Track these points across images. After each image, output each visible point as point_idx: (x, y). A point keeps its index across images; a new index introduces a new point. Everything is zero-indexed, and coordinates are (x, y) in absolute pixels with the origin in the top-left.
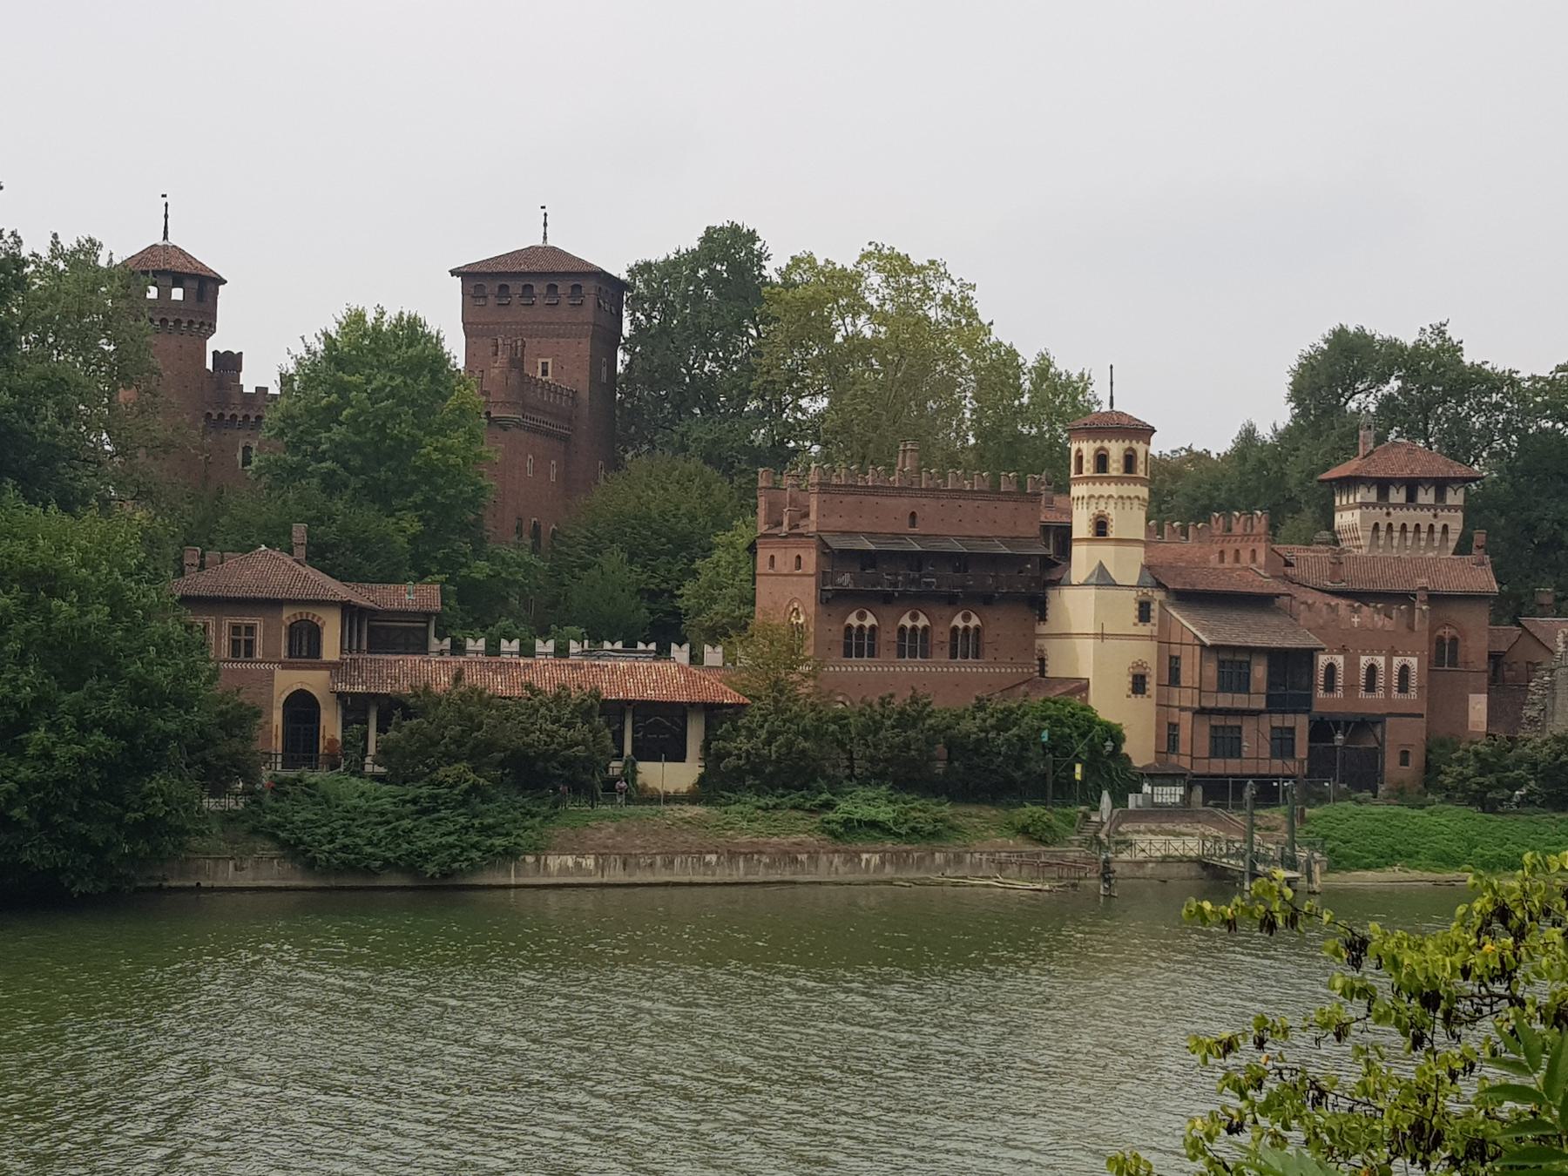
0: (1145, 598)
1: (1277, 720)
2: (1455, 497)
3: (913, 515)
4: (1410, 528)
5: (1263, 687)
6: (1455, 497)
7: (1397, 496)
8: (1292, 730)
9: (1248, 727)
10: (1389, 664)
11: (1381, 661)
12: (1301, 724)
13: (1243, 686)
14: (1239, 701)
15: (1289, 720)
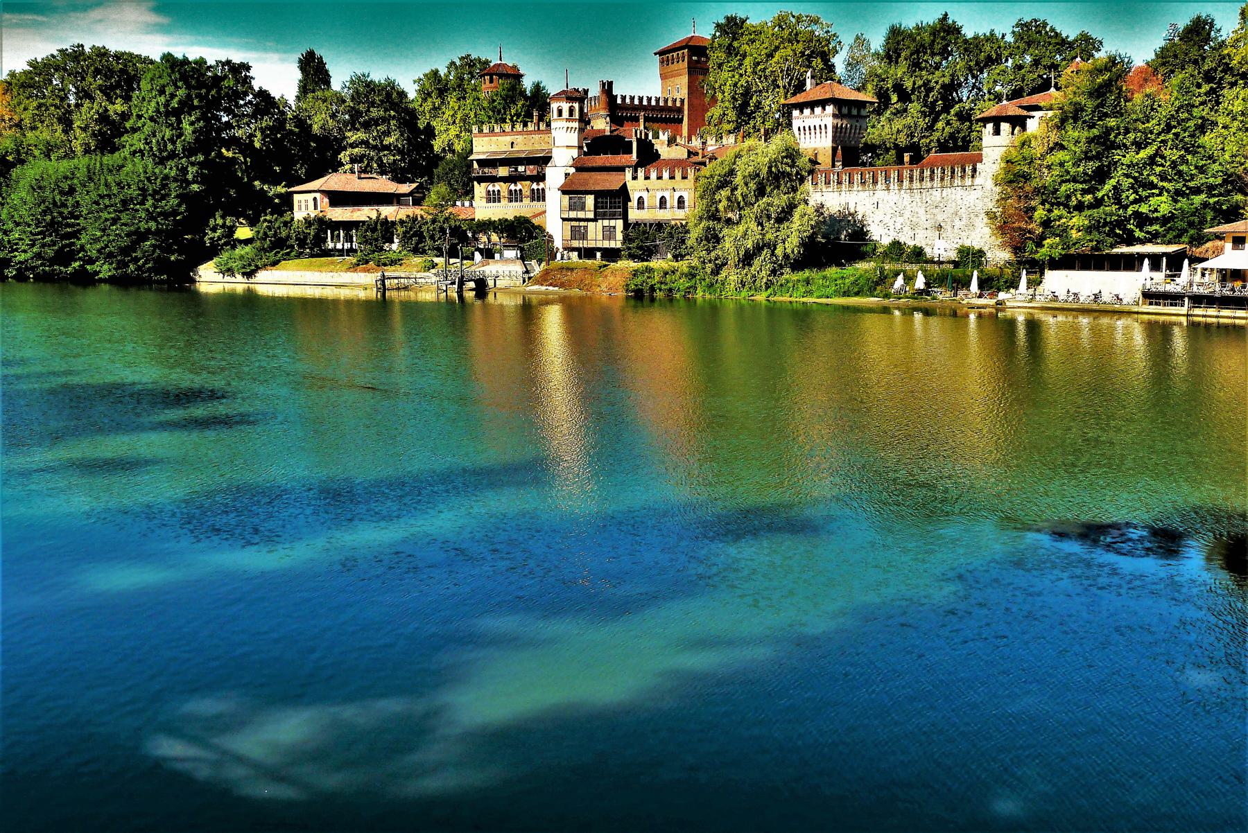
0: (567, 172)
1: (606, 223)
2: (830, 109)
3: (512, 143)
4: (812, 128)
5: (592, 208)
6: (830, 109)
7: (807, 111)
8: (614, 227)
9: (591, 225)
10: (672, 197)
11: (667, 195)
12: (619, 224)
13: (583, 208)
14: (581, 215)
15: (613, 223)
